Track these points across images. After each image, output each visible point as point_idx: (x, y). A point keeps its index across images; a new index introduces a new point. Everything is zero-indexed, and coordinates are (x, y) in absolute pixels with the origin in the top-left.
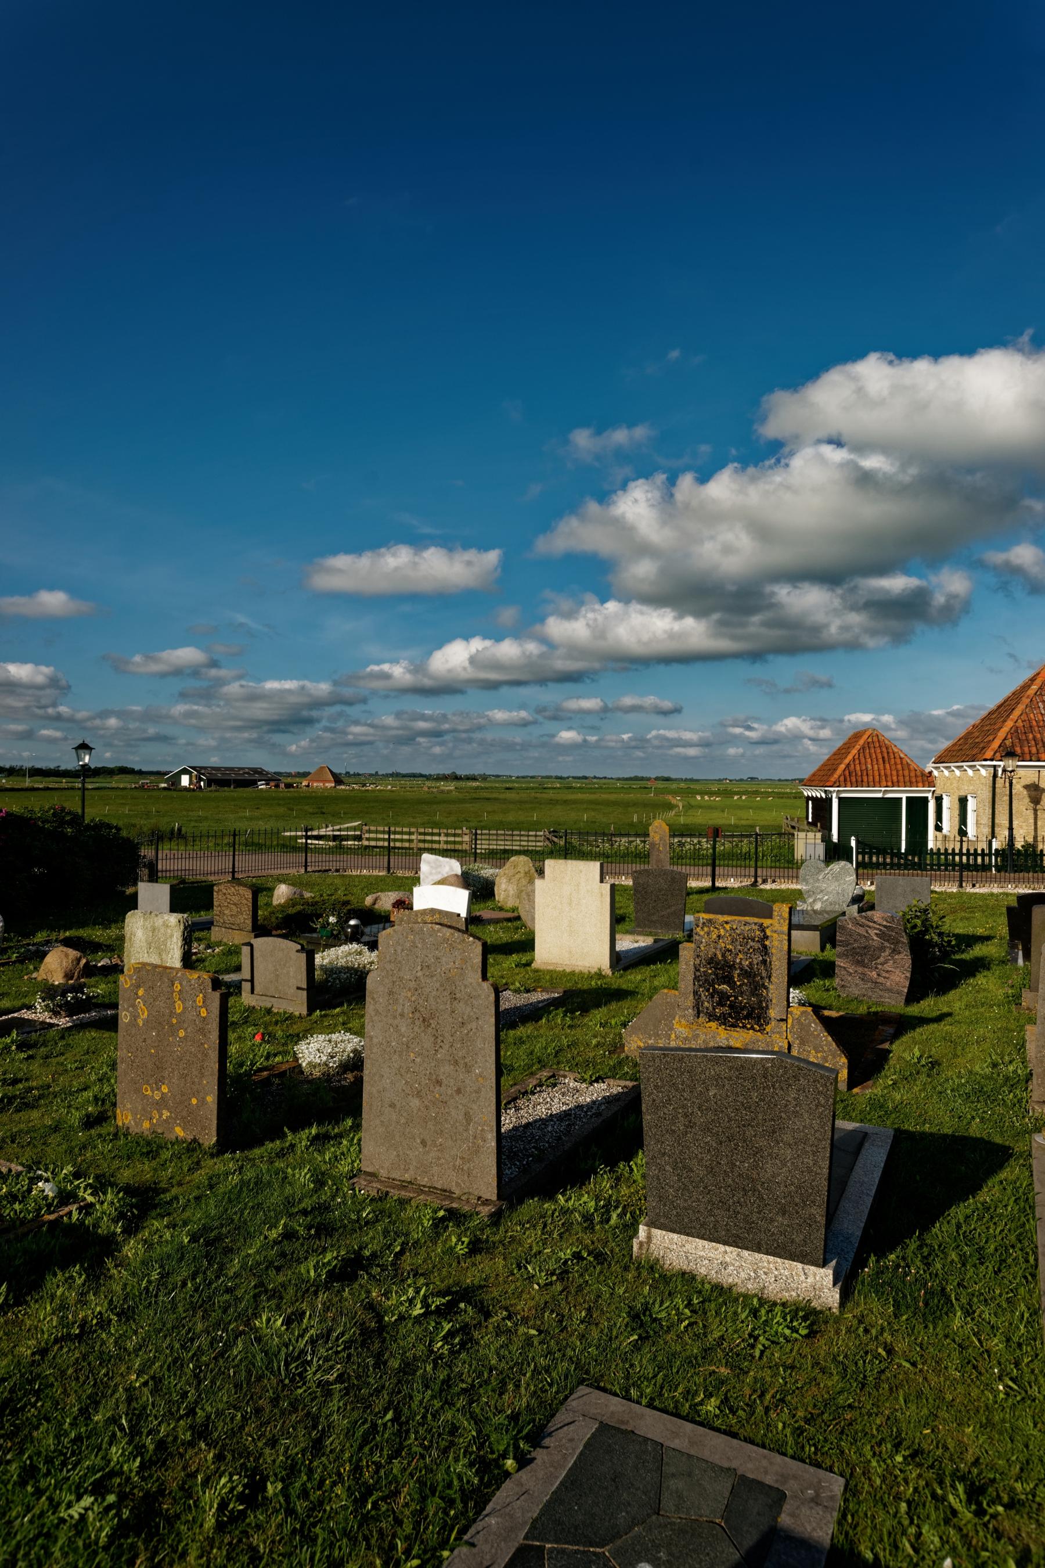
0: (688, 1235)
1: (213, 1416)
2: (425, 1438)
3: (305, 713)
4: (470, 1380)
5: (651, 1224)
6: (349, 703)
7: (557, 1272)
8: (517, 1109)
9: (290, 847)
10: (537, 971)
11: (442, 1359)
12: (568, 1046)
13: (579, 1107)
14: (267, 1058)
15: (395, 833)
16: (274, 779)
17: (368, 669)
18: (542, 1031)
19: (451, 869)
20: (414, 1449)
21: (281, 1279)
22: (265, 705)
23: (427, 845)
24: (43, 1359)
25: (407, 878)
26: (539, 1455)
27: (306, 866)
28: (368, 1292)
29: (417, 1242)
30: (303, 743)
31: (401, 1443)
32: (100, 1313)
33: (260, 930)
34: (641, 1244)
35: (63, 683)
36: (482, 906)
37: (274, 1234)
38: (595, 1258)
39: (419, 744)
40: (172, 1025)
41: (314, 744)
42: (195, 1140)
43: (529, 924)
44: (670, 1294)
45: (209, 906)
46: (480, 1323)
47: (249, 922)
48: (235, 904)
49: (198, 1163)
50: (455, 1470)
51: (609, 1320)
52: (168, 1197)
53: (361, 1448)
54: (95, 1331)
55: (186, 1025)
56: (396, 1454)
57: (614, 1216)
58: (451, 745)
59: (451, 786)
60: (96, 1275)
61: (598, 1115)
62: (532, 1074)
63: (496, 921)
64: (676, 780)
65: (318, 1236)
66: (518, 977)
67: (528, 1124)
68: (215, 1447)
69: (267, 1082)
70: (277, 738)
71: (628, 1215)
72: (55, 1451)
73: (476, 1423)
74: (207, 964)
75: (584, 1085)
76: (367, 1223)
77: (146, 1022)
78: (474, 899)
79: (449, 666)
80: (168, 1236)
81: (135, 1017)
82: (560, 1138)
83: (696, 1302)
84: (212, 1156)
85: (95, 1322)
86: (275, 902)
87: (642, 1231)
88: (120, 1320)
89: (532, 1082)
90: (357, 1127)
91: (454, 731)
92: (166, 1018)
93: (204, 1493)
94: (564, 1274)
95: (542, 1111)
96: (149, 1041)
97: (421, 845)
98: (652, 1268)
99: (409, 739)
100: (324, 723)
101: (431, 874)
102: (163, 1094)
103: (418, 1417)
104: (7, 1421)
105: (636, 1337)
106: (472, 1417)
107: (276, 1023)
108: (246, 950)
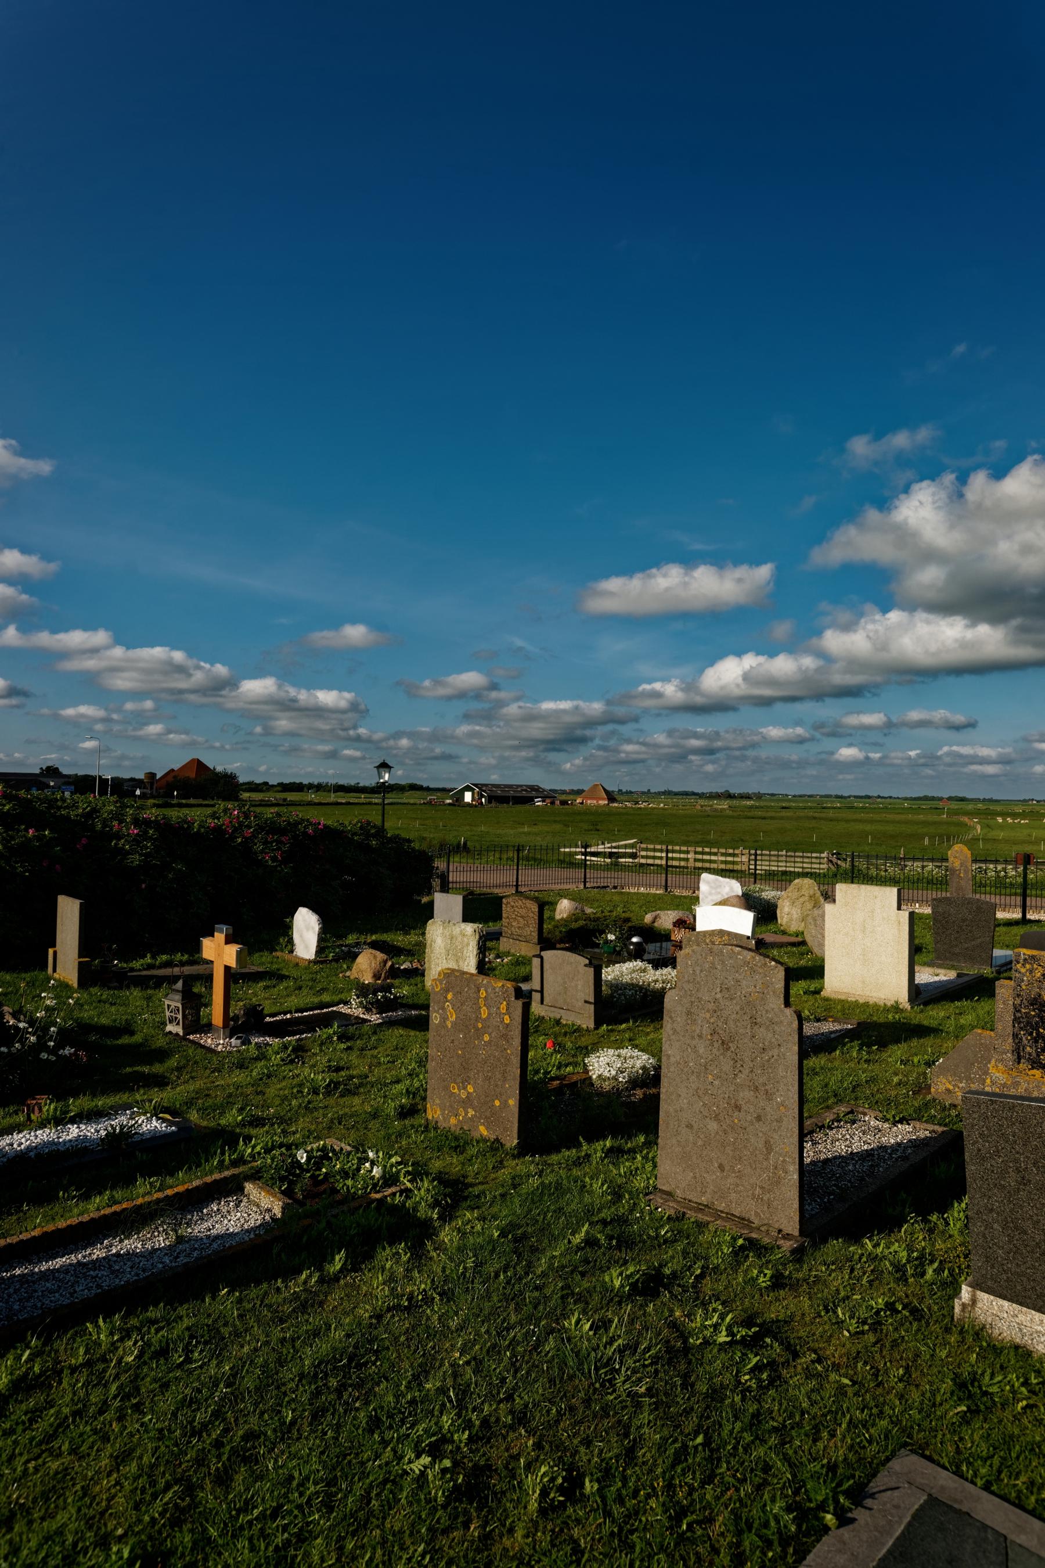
0: (1021, 1304)
1: (530, 1405)
2: (737, 1471)
3: (579, 733)
4: (780, 1419)
5: (976, 1286)
6: (621, 722)
7: (869, 1321)
8: (815, 1143)
9: (568, 862)
10: (827, 999)
11: (750, 1392)
12: (867, 1082)
13: (883, 1148)
14: (559, 1068)
15: (673, 851)
16: (549, 796)
17: (640, 689)
18: (837, 1063)
19: (732, 889)
20: (727, 1479)
21: (586, 1284)
22: (541, 725)
23: (707, 865)
24: (378, 1322)
25: (685, 897)
26: (859, 1514)
27: (585, 882)
28: (671, 1311)
29: (716, 1268)
30: (577, 762)
31: (713, 1471)
32: (424, 1290)
33: (546, 943)
34: (964, 1306)
35: (362, 707)
36: (764, 928)
37: (577, 1239)
38: (912, 1312)
39: (691, 761)
40: (477, 1029)
41: (588, 763)
42: (497, 1140)
43: (816, 950)
44: (1002, 1367)
45: (497, 916)
46: (788, 1361)
47: (535, 934)
48: (522, 917)
49: (501, 1162)
50: (771, 1510)
51: (931, 1383)
52: (476, 1190)
53: (673, 1466)
54: (421, 1306)
55: (490, 1030)
56: (708, 1480)
57: (930, 1271)
58: (723, 763)
59: (724, 805)
60: (418, 1254)
61: (905, 1158)
62: (828, 1108)
63: (781, 945)
64: (972, 800)
65: (619, 1247)
66: (806, 1005)
67: (827, 1161)
68: (534, 1436)
69: (559, 1091)
70: (552, 756)
71: (946, 1272)
72: (394, 1409)
73: (790, 1466)
74: (497, 972)
75: (886, 1125)
76: (666, 1241)
77: (454, 1024)
78: (758, 922)
79: (723, 682)
80: (479, 1227)
81: (444, 1019)
82: (862, 1179)
83: (1034, 1381)
84: (514, 1157)
85: (420, 1297)
86: (558, 917)
87: (966, 1293)
88: (441, 1300)
89: (829, 1117)
90: (652, 1143)
91: (728, 748)
92: (472, 1022)
93: (527, 1477)
94: (876, 1326)
95: (841, 1148)
96: (456, 1043)
97: (699, 865)
98: (977, 1334)
99: (681, 757)
100: (597, 742)
101: (710, 894)
102: (469, 1093)
103: (729, 1447)
104: (354, 1373)
105: (965, 1408)
106: (785, 1458)
107: (565, 1034)
108: (536, 962)
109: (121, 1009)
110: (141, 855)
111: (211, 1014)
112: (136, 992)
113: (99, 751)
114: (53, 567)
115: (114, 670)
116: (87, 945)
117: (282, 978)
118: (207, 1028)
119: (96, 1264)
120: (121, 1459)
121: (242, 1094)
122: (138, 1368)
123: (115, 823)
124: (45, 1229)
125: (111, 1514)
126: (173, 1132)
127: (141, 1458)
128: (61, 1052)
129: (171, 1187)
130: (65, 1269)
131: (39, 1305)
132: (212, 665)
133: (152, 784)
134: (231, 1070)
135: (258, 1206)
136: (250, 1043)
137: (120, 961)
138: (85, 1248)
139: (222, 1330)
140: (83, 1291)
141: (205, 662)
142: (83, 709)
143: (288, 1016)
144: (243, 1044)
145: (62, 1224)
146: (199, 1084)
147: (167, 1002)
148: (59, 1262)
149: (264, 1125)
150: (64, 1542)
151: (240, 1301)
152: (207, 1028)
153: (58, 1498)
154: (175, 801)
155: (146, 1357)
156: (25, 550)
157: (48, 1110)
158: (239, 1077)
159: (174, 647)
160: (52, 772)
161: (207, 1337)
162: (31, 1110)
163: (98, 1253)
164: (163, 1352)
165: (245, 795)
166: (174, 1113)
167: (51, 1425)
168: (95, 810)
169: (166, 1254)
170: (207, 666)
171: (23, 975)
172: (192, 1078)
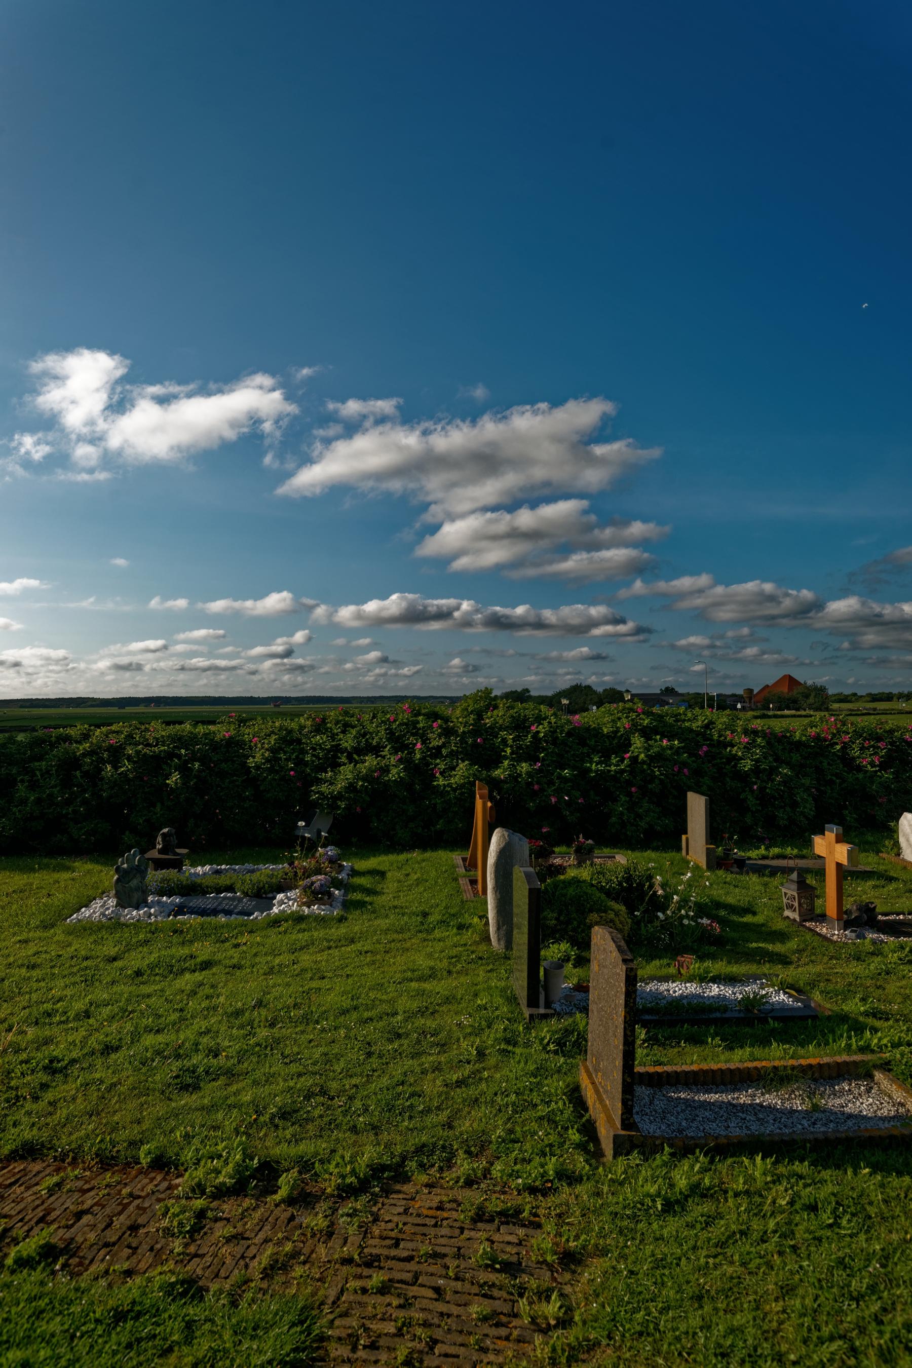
109: (743, 891)
110: (752, 760)
111: (825, 906)
112: (754, 878)
113: (706, 673)
114: (667, 529)
115: (717, 605)
116: (714, 834)
117: (891, 879)
118: (822, 918)
119: (743, 1108)
120: (787, 1291)
121: (861, 985)
122: (791, 1213)
123: (728, 733)
124: (701, 1067)
125: (782, 1337)
126: (799, 1008)
127: (803, 1298)
128: (699, 920)
129: (803, 1057)
130: (720, 1105)
131: (702, 1128)
132: (798, 591)
133: (750, 699)
134: (848, 960)
135: (890, 1097)
136: (865, 938)
137: (739, 849)
138: (733, 1091)
139: (868, 1208)
140: (736, 1131)
141: (792, 589)
142: (692, 639)
143: (901, 917)
144: (858, 937)
145: (714, 1066)
146: (819, 968)
147: (784, 890)
148: (713, 1097)
149: (887, 1019)
150: (745, 1341)
151: (882, 1185)
152: (822, 918)
153: (736, 1299)
154: (771, 713)
155: (797, 1206)
156: (645, 520)
157: (694, 968)
158: (855, 968)
159: (765, 580)
160: (669, 691)
161: (853, 1209)
162: (681, 965)
163: (743, 1098)
164: (813, 1208)
165: (836, 706)
166: (799, 991)
167: (723, 1234)
168: (711, 723)
169: (804, 1118)
170: (794, 592)
171: (664, 855)
172: (812, 962)
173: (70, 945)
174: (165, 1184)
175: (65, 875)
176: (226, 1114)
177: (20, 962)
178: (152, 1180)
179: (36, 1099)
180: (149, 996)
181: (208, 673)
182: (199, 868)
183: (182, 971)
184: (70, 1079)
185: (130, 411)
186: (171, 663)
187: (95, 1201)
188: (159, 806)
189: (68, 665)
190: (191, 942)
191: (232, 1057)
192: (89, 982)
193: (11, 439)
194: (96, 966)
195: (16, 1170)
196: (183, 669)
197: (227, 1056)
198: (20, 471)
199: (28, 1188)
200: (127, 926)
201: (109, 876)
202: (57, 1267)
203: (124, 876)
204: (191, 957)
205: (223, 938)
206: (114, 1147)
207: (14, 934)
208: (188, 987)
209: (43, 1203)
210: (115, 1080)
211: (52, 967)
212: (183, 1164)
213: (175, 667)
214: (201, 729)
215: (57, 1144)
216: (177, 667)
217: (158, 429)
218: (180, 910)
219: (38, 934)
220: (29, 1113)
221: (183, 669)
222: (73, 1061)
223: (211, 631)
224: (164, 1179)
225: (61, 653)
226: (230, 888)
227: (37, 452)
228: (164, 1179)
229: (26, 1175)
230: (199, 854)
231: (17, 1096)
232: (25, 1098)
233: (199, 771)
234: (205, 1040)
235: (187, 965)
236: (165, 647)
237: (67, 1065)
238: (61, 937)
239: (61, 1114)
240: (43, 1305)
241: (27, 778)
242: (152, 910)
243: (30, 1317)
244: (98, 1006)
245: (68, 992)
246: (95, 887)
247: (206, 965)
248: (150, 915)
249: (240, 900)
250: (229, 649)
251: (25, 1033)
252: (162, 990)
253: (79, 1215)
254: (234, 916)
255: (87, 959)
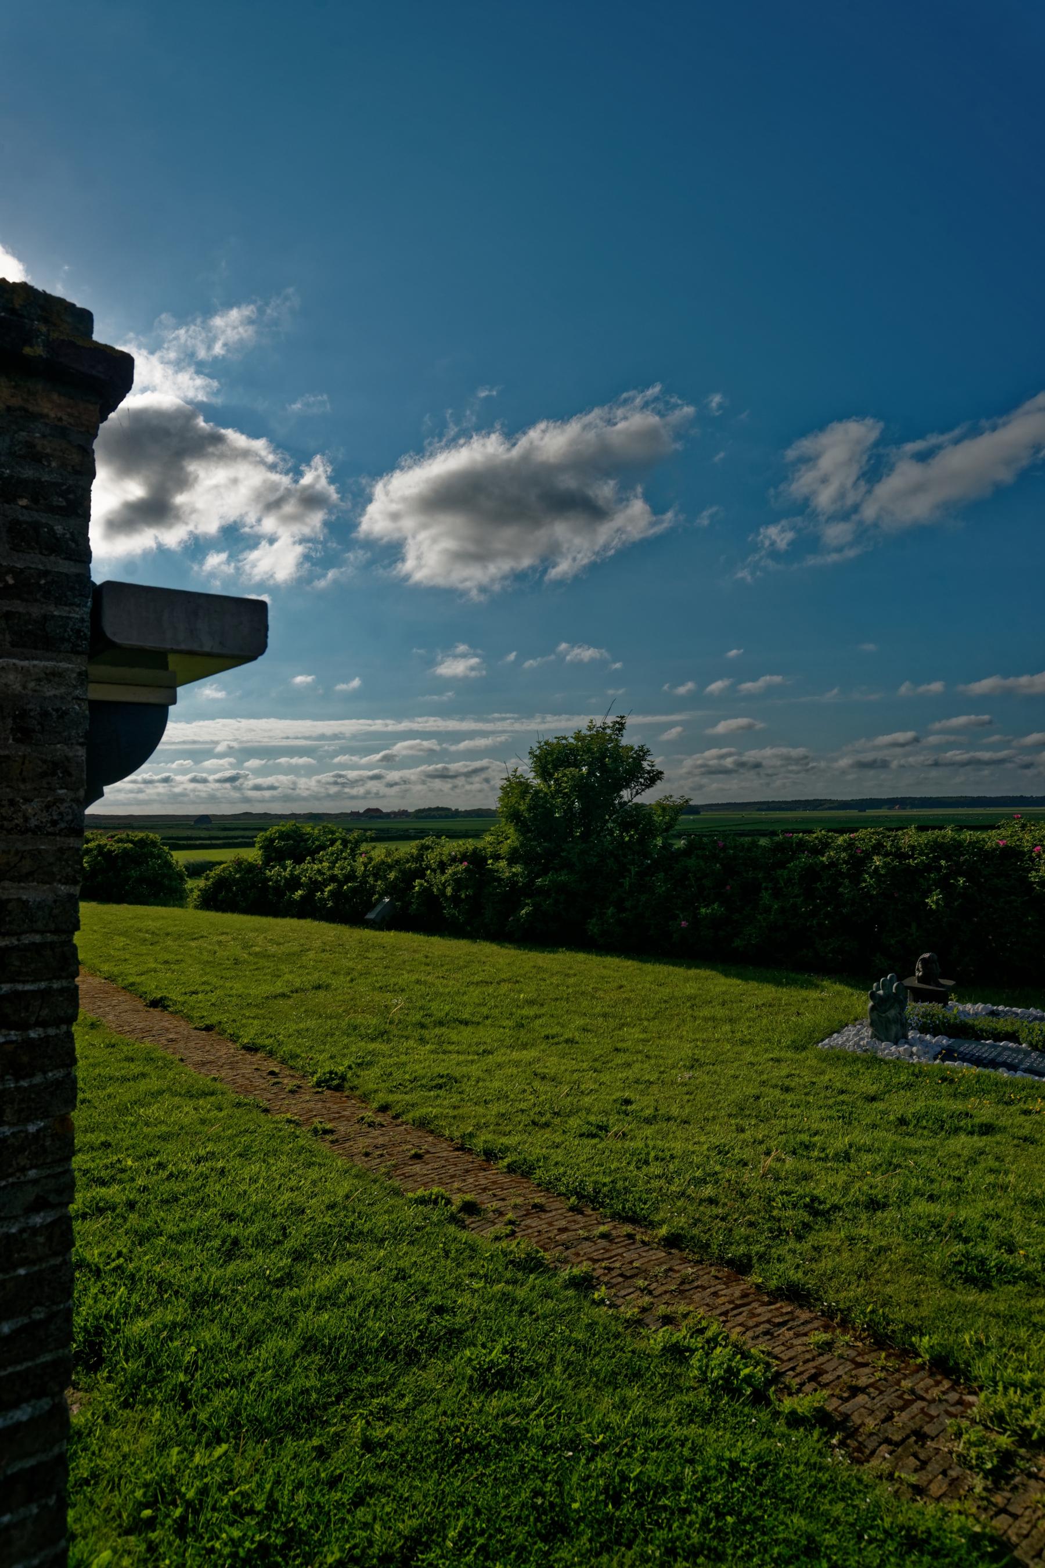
173: (823, 1073)
174: (953, 1397)
175: (814, 994)
176: (1031, 1335)
177: (774, 1081)
178: (938, 1383)
179: (799, 1238)
180: (916, 1152)
181: (968, 768)
182: (969, 1006)
183: (957, 1130)
184: (834, 1227)
185: (888, 475)
186: (922, 758)
187: (872, 1380)
188: (914, 926)
189: (807, 764)
190: (965, 1096)
191: (1034, 1260)
192: (848, 1120)
193: (758, 534)
194: (853, 1102)
195: (784, 1310)
196: (936, 764)
197: (1026, 1257)
198: (770, 564)
199: (797, 1335)
200: (886, 1063)
201: (861, 1002)
202: (834, 1441)
203: (880, 1005)
204: (967, 1114)
205: (1006, 1099)
206: (888, 1324)
207: (766, 1051)
208: (965, 1152)
209: (813, 1359)
210: (883, 1243)
211: (806, 1094)
212: (976, 1379)
213: (927, 763)
214: (967, 835)
215: (825, 1297)
216: (930, 762)
217: (918, 489)
218: (948, 1054)
219: (789, 1054)
220: (793, 1251)
221: (936, 764)
222: (836, 1208)
223: (973, 717)
224: (952, 1388)
225: (801, 751)
226: (1013, 1037)
227: (782, 540)
228: (952, 1388)
229: (793, 1320)
230: (968, 991)
231: (779, 1227)
232: (788, 1233)
233: (965, 888)
234: (994, 1226)
235: (962, 1123)
236: (916, 740)
237: (830, 1209)
238: (814, 1062)
239: (826, 1264)
240: (824, 1480)
241: (770, 885)
242: (914, 1049)
243: (810, 1486)
244: (859, 1150)
245: (824, 1126)
246: (846, 1010)
247: (987, 1129)
248: (911, 1055)
249: (1027, 1054)
250: (996, 738)
251: (784, 1161)
252: (933, 1149)
253: (855, 1391)
254: (1019, 1074)
255: (842, 1092)
